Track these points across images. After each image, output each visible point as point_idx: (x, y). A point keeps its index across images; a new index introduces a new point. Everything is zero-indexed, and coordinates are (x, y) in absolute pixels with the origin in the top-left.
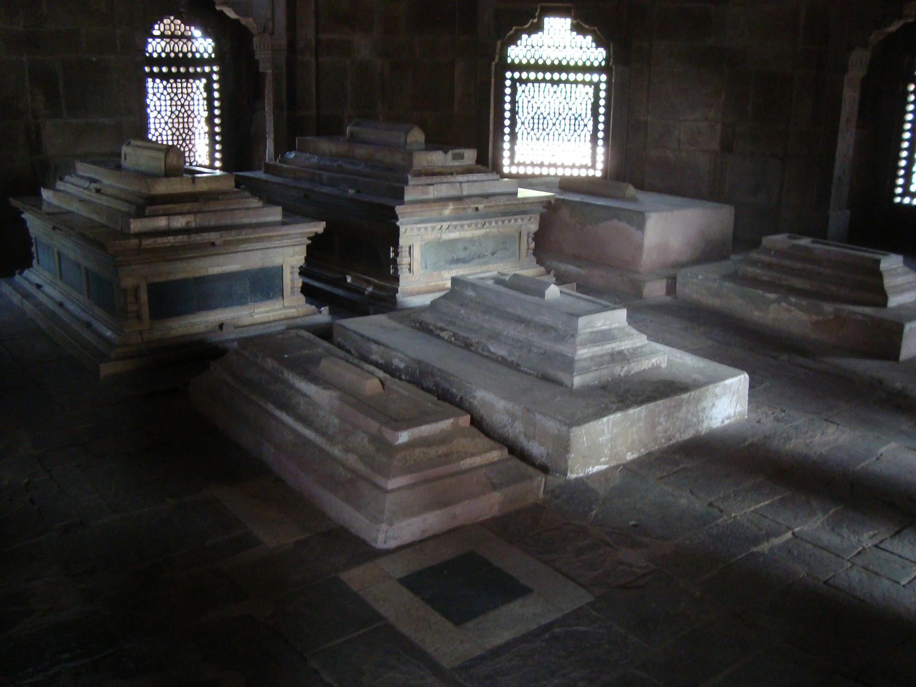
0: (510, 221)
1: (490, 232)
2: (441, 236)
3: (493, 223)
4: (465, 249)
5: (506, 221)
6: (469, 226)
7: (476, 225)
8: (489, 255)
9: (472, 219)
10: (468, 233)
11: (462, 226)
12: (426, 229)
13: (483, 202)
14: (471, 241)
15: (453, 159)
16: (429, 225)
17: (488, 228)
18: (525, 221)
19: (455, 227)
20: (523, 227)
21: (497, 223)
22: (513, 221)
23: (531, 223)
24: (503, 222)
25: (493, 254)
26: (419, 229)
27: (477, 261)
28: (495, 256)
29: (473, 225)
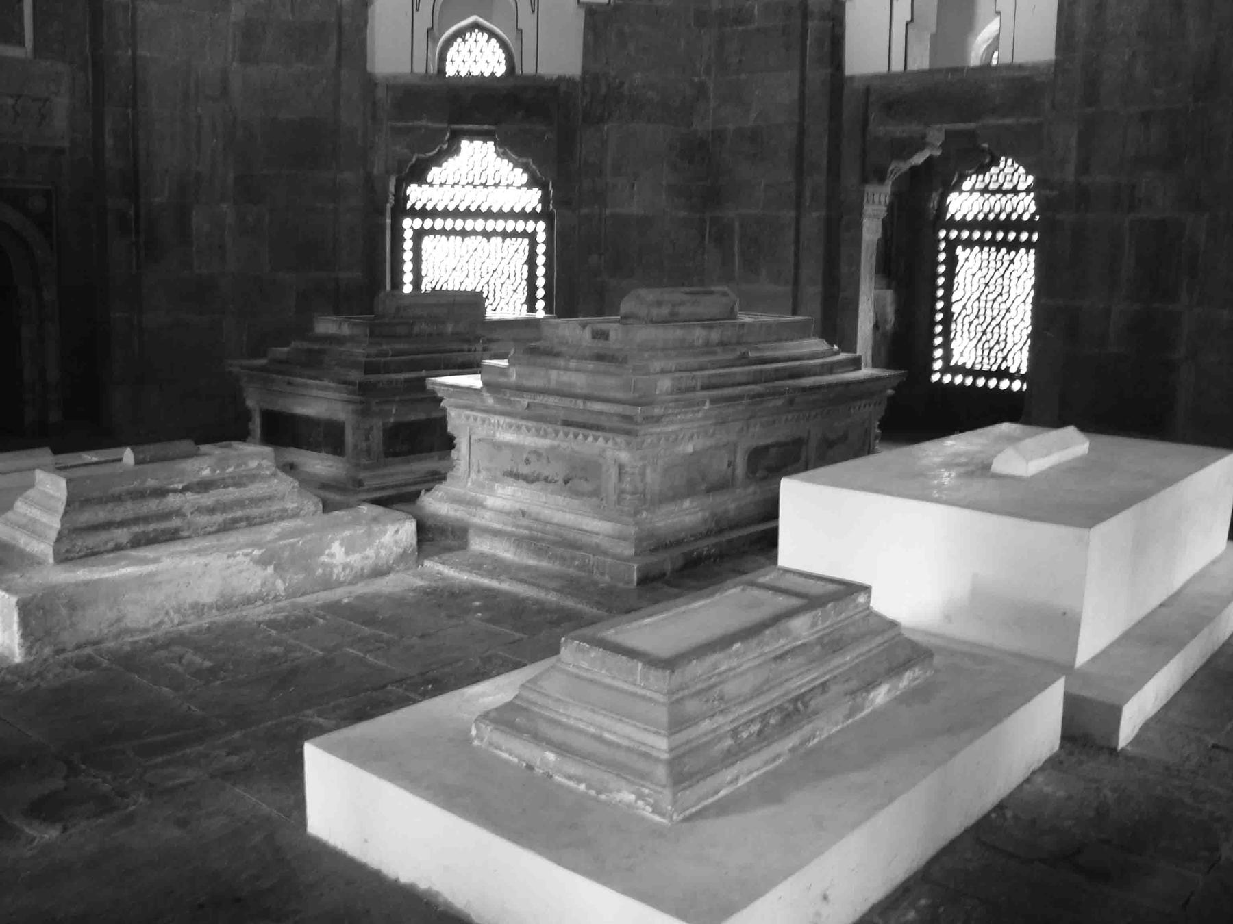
0: (586, 437)
1: (559, 446)
2: (494, 433)
3: (561, 434)
4: (527, 462)
5: (580, 437)
6: (529, 429)
7: (538, 430)
8: (561, 482)
9: (523, 418)
10: (530, 440)
11: (519, 427)
12: (476, 419)
13: (525, 396)
14: (536, 452)
15: (594, 338)
16: (480, 415)
17: (553, 439)
18: (610, 443)
19: (511, 426)
20: (609, 453)
21: (566, 434)
22: (590, 439)
23: (619, 450)
24: (576, 436)
25: (566, 482)
26: (468, 417)
27: (539, 485)
28: (569, 485)
29: (534, 430)
